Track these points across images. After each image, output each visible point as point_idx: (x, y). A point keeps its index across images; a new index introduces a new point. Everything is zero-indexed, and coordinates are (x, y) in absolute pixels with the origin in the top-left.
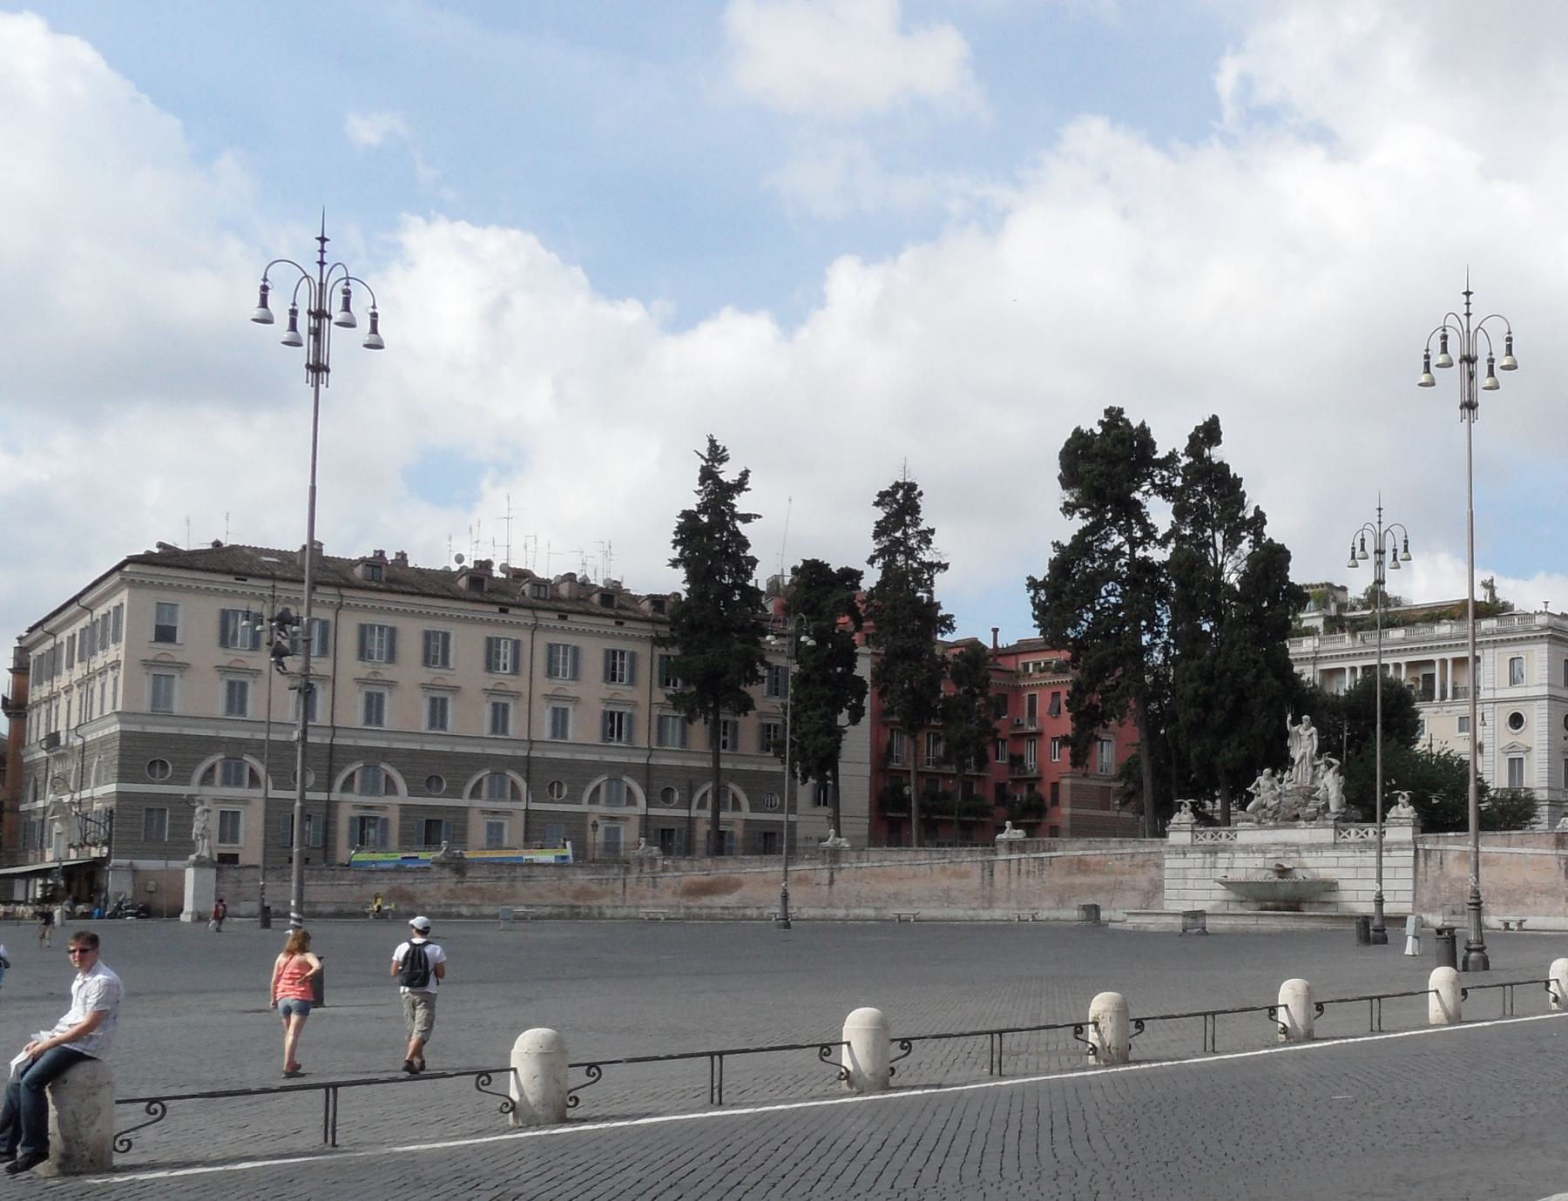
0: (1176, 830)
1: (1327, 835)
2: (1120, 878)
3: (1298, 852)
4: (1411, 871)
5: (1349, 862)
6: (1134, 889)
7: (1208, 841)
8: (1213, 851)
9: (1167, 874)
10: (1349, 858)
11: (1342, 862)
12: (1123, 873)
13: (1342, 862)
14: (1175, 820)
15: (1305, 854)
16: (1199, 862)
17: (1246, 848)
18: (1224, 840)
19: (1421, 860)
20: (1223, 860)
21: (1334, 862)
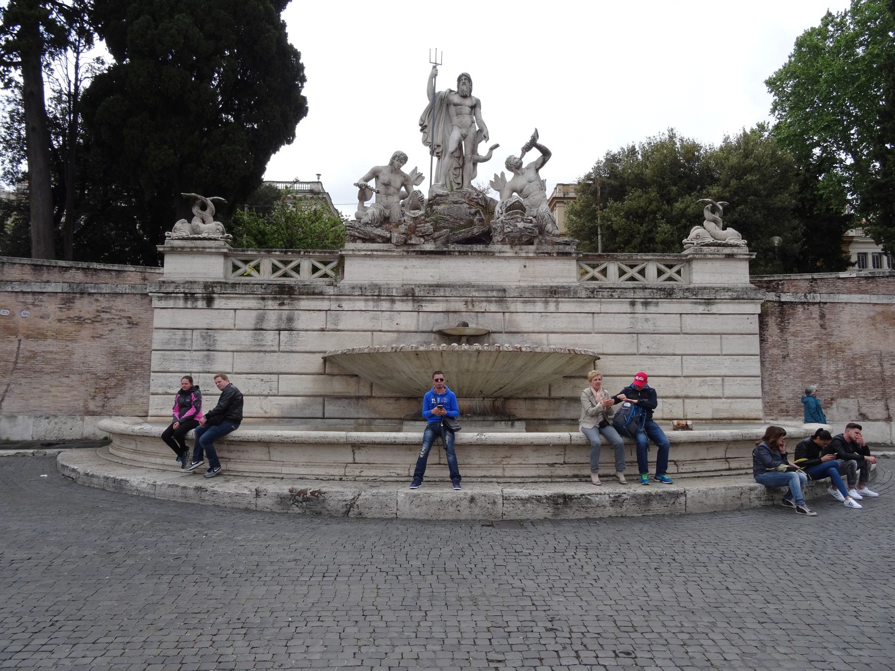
0: (174, 250)
1: (564, 272)
2: (29, 345)
3: (501, 300)
4: (757, 339)
5: (623, 323)
6: (65, 369)
7: (266, 275)
8: (285, 293)
9: (158, 339)
10: (615, 315)
11: (602, 322)
12: (41, 335)
13: (602, 322)
14: (182, 227)
15: (520, 307)
16: (248, 319)
17: (376, 293)
18: (305, 276)
19: (772, 322)
20: (309, 315)
21: (585, 323)
